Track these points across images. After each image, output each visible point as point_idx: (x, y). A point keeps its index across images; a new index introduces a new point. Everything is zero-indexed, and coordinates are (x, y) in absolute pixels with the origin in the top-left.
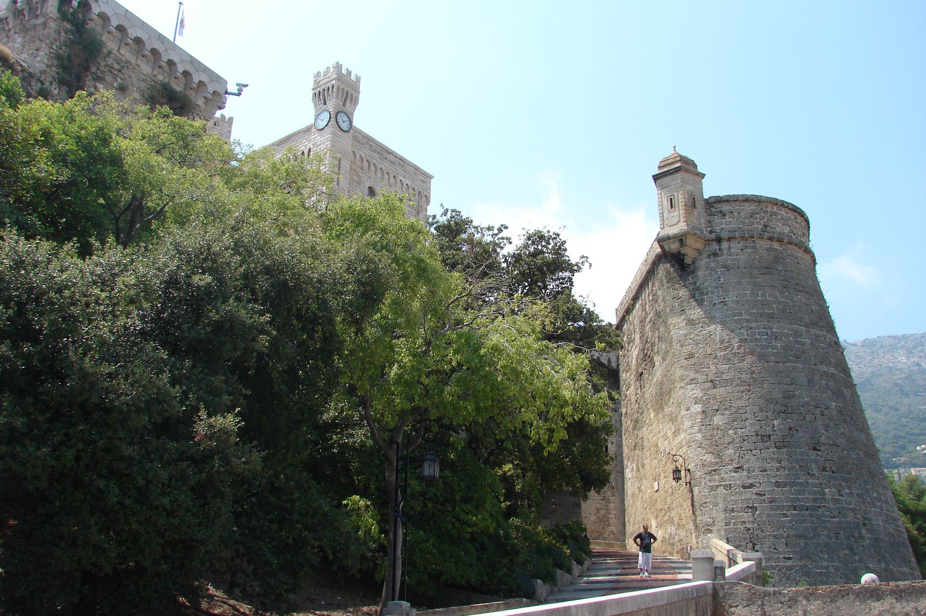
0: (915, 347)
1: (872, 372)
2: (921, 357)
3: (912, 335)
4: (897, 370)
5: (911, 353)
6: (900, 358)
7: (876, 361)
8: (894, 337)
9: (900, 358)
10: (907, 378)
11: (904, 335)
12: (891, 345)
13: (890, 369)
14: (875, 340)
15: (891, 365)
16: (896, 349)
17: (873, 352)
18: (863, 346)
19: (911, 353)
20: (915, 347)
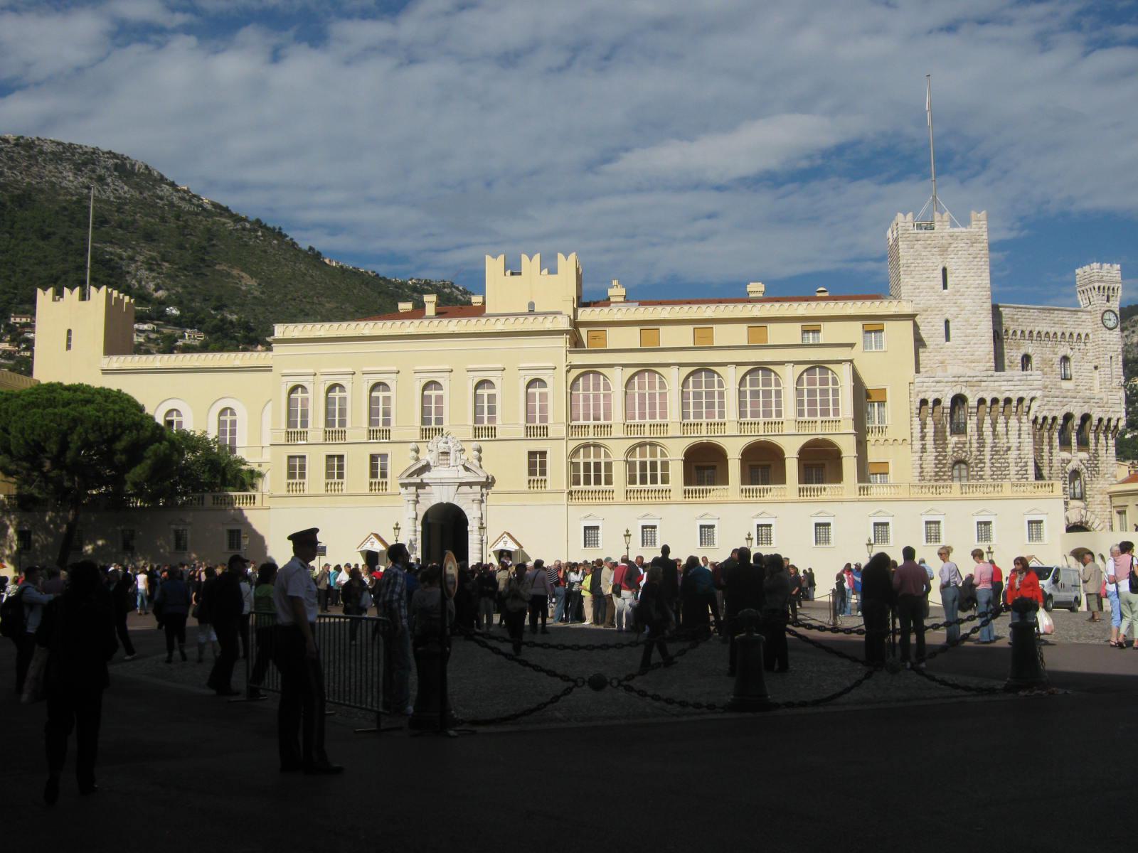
0: (85, 164)
1: (29, 184)
2: (91, 178)
3: (81, 147)
4: (62, 188)
5: (81, 171)
6: (65, 174)
7: (35, 170)
8: (59, 144)
9: (65, 174)
10: (75, 202)
11: (71, 144)
12: (53, 153)
13: (53, 184)
14: (33, 142)
15: (53, 179)
16: (61, 160)
17: (30, 157)
18: (16, 145)
19: (81, 171)
20: (85, 164)
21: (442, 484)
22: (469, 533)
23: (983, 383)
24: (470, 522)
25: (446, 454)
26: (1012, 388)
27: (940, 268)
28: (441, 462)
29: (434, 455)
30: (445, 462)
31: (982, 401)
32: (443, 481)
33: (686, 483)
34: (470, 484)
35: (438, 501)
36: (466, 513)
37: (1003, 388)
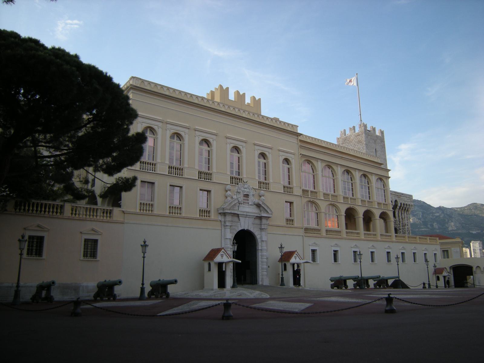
21: (246, 216)
22: (260, 251)
23: (401, 197)
24: (260, 244)
25: (247, 196)
26: (407, 200)
27: (375, 148)
28: (244, 201)
29: (241, 198)
30: (246, 201)
31: (401, 204)
32: (248, 214)
33: (347, 228)
34: (260, 218)
35: (242, 228)
36: (258, 237)
37: (406, 200)
